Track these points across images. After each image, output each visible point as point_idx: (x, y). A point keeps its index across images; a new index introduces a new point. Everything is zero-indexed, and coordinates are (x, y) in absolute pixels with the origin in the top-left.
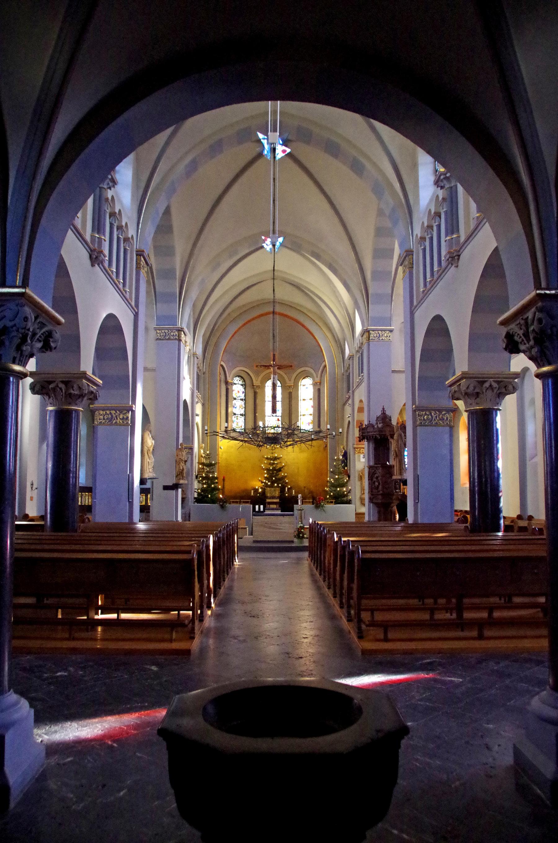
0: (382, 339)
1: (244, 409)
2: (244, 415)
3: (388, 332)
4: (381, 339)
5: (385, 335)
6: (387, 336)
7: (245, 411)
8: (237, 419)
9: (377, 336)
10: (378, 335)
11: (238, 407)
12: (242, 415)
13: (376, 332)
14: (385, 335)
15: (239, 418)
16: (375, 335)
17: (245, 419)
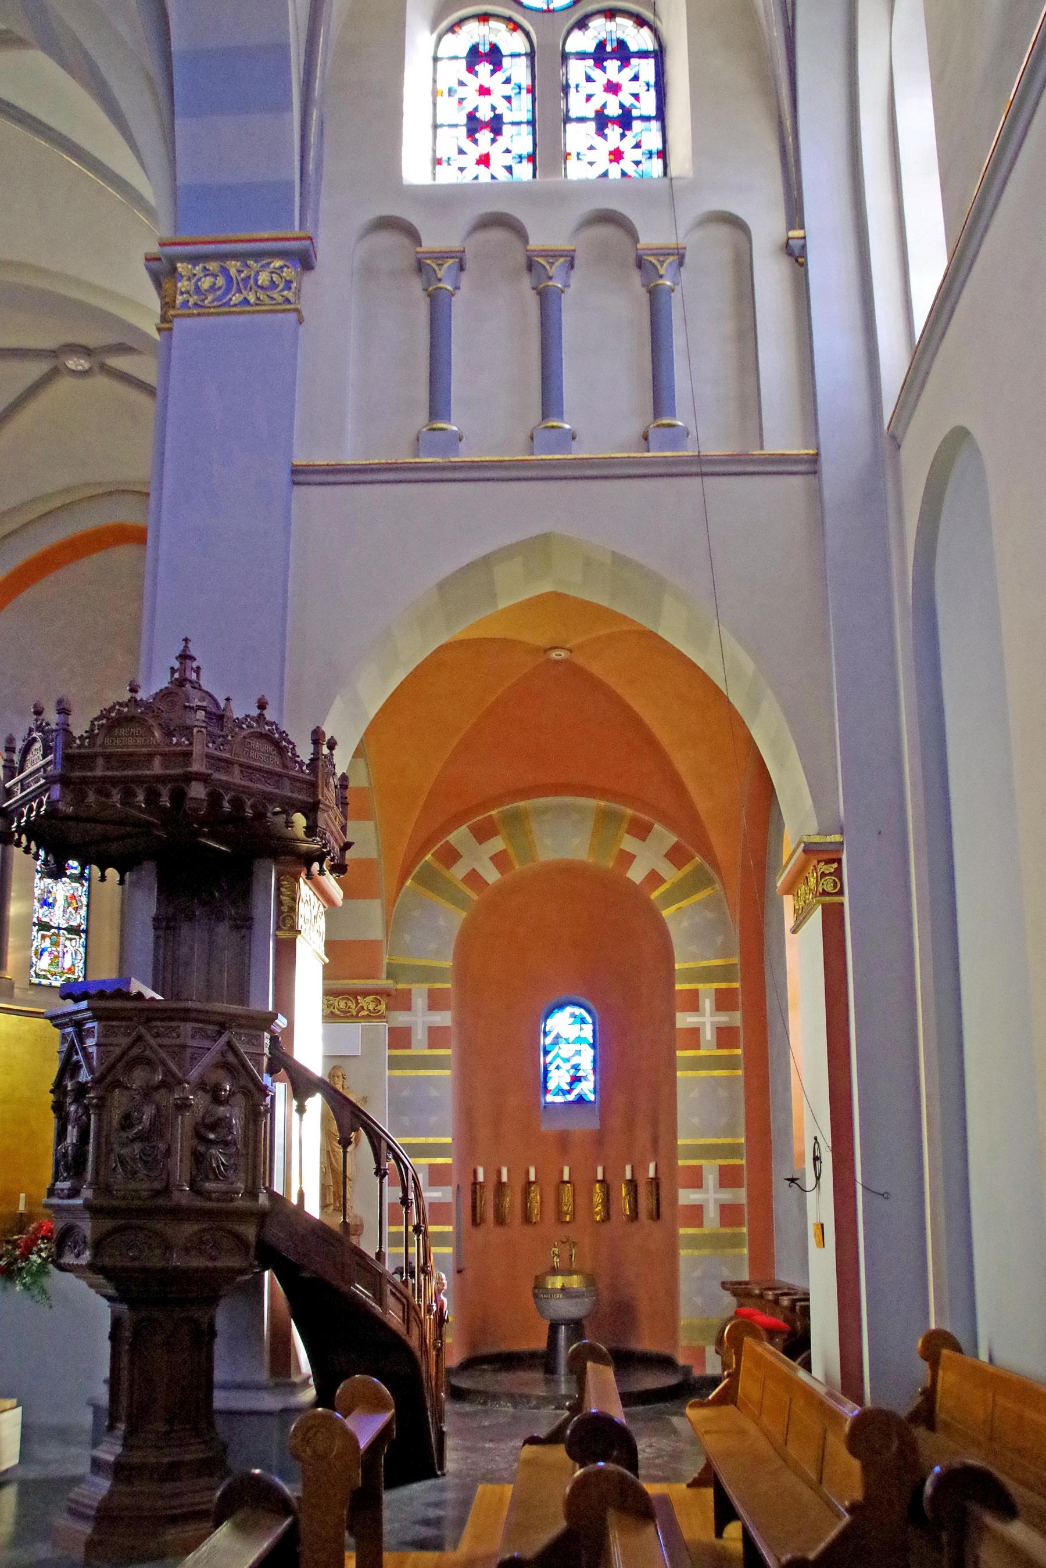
0: (246, 302)
1: (83, 912)
2: (85, 932)
3: (278, 263)
4: (236, 298)
5: (263, 278)
6: (273, 285)
7: (88, 918)
8: (55, 944)
9: (213, 288)
10: (221, 281)
11: (60, 904)
12: (73, 930)
13: (213, 266)
14: (263, 278)
15: (62, 939)
16: (206, 283)
17: (86, 947)
